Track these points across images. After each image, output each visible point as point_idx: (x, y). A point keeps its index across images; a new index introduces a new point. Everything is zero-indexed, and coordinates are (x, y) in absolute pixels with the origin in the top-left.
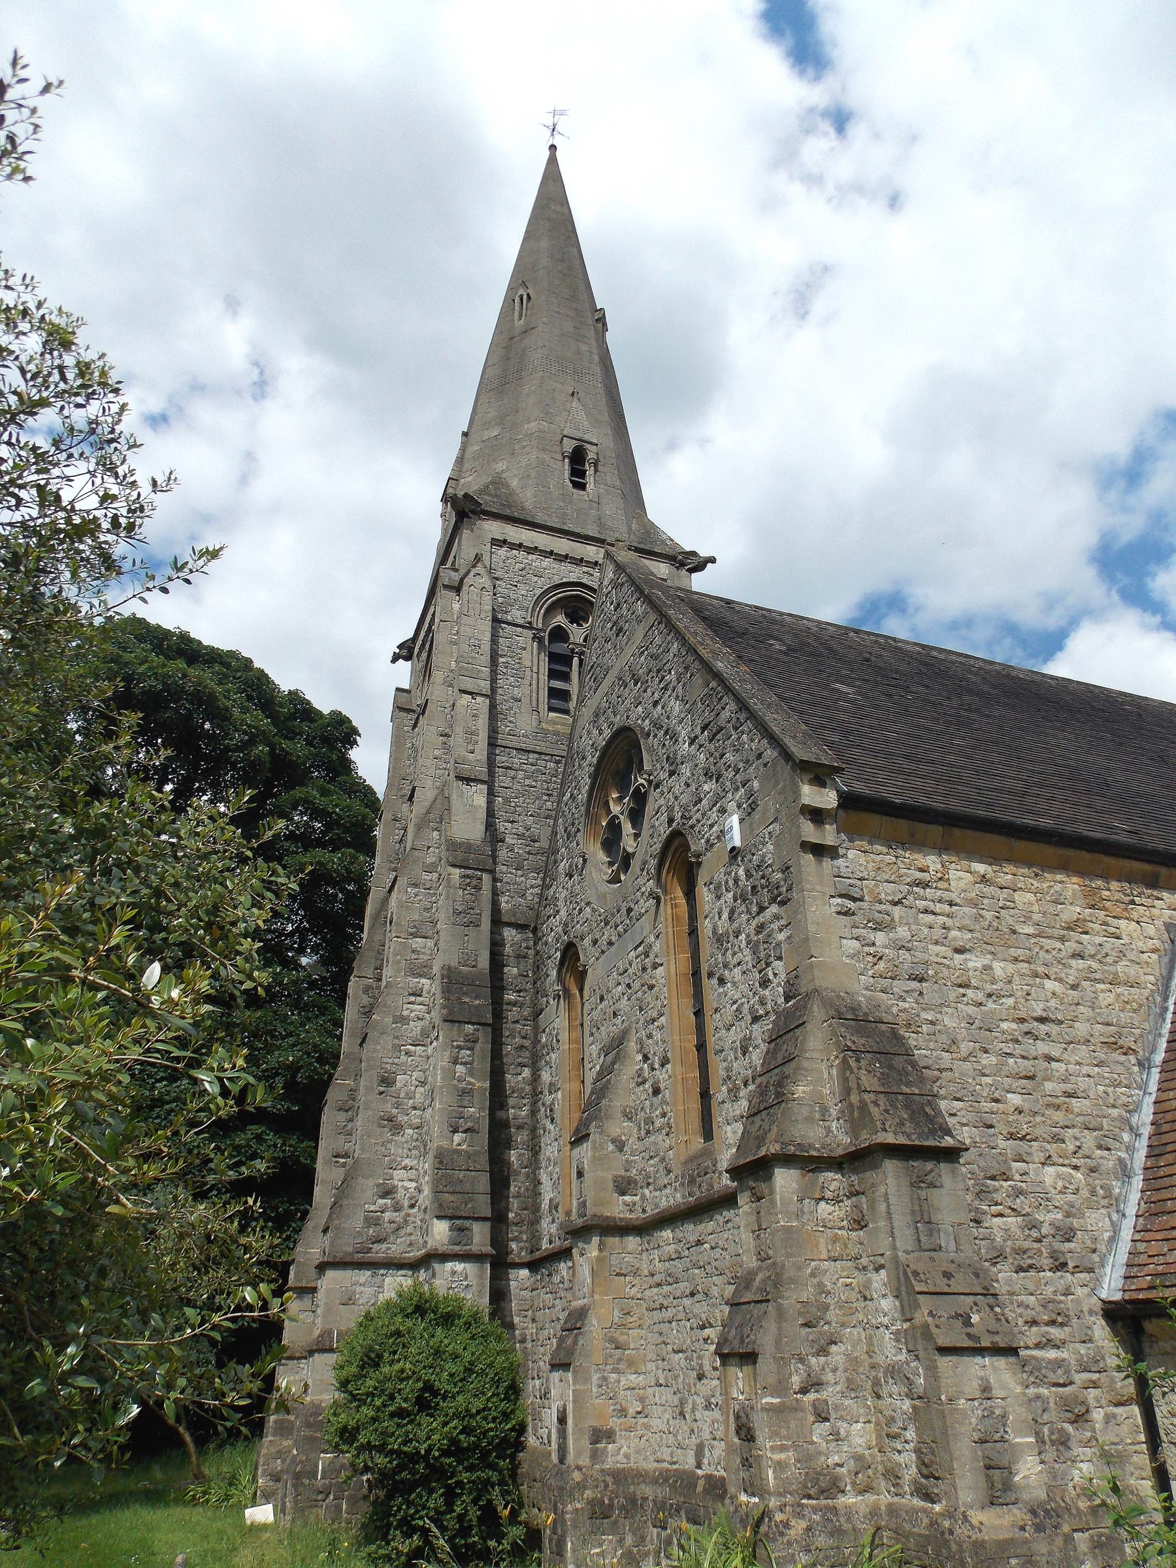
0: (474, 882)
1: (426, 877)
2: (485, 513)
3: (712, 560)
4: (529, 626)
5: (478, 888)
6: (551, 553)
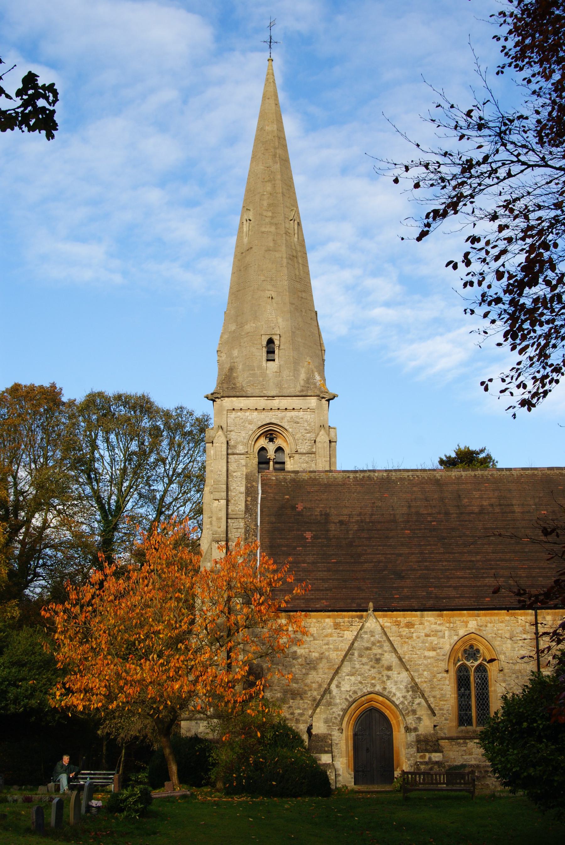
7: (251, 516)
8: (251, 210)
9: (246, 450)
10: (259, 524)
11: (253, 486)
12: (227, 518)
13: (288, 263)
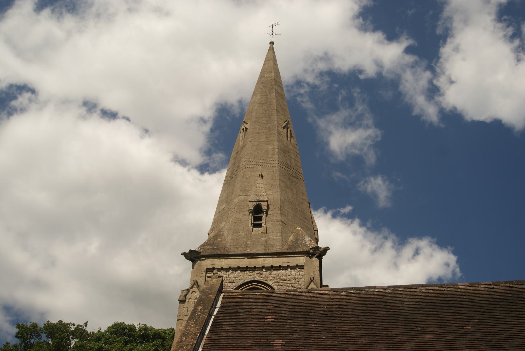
8: (249, 123)
13: (278, 152)
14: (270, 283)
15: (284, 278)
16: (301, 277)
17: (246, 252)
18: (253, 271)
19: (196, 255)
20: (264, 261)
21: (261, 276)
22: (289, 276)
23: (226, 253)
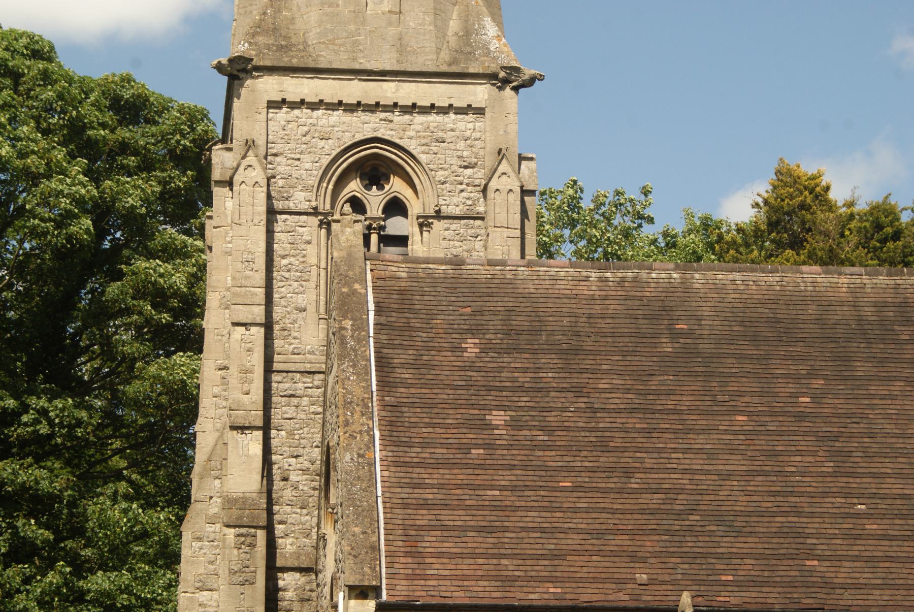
0: (249, 540)
1: (209, 528)
2: (257, 68)
3: (541, 78)
4: (315, 212)
5: (252, 546)
6: (340, 103)
7: (354, 366)
9: (314, 204)
10: (374, 388)
11: (354, 292)
12: (268, 370)
14: (411, 146)
15: (441, 134)
16: (478, 135)
17: (357, 67)
18: (373, 112)
19: (243, 66)
20: (397, 90)
21: (391, 125)
22: (453, 130)
23: (312, 65)
